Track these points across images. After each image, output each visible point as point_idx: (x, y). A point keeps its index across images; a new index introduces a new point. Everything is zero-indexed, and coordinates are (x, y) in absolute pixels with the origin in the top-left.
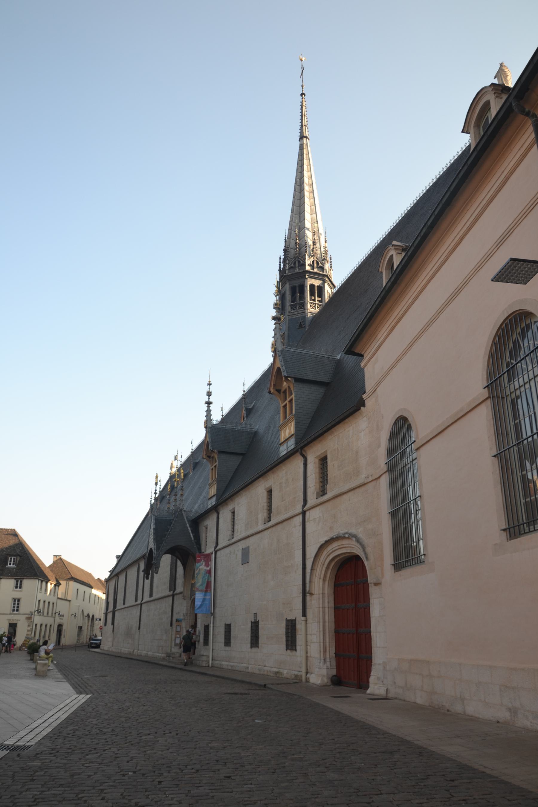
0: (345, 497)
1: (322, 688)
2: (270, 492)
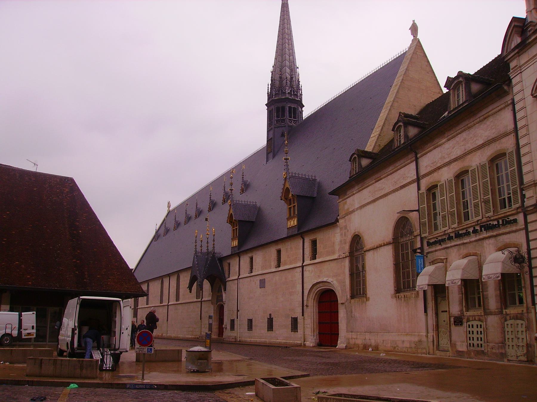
0: (327, 263)
1: (313, 347)
2: (279, 252)
